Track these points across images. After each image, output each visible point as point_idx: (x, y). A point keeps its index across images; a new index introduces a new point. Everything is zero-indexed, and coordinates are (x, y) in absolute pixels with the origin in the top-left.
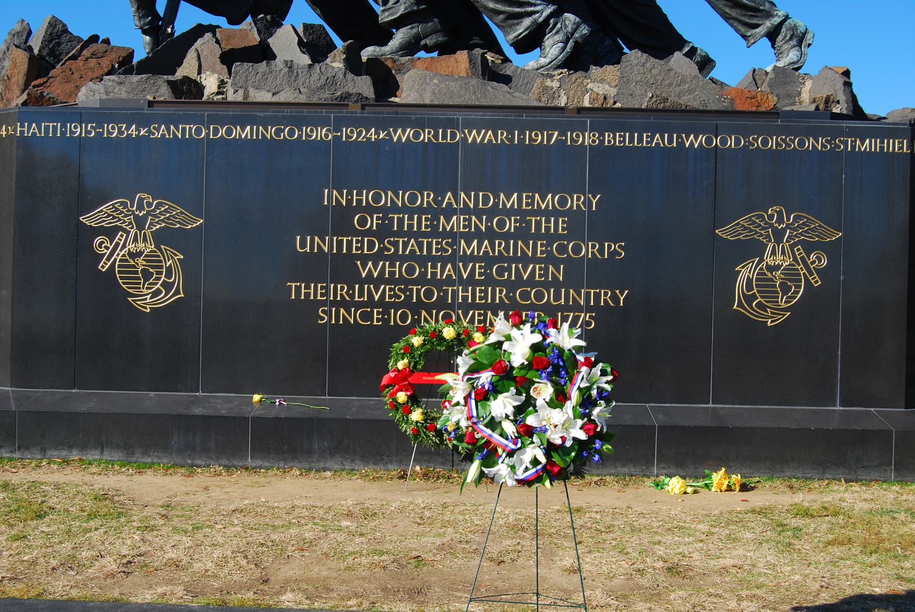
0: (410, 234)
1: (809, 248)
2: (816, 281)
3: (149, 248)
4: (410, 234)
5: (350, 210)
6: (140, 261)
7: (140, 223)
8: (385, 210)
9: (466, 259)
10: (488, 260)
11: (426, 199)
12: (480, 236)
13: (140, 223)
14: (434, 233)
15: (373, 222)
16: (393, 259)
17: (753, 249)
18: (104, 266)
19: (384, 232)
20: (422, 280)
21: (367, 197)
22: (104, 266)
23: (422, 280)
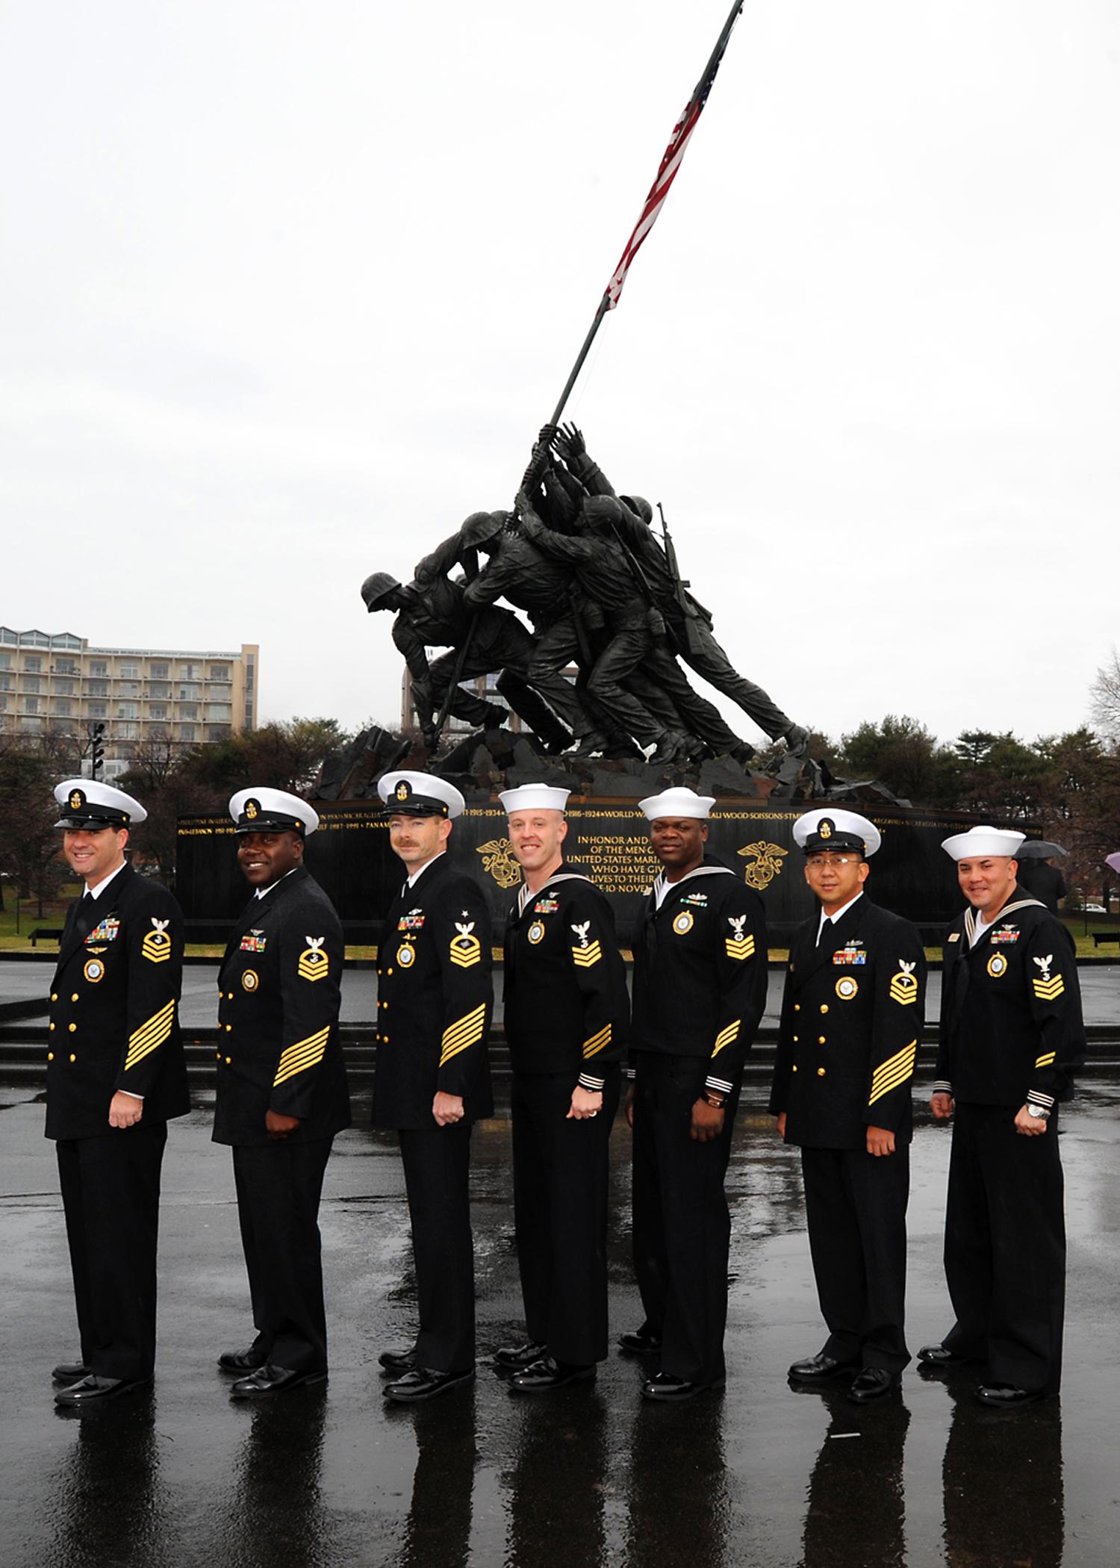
0: (614, 854)
1: (775, 858)
2: (778, 872)
3: (507, 860)
4: (614, 854)
5: (590, 845)
6: (502, 867)
7: (502, 851)
8: (604, 845)
9: (638, 864)
10: (646, 865)
11: (621, 840)
12: (643, 855)
13: (502, 851)
14: (624, 854)
15: (599, 850)
16: (607, 865)
17: (753, 859)
18: (487, 869)
19: (603, 853)
20: (619, 873)
21: (596, 840)
22: (487, 869)
23: (619, 873)
